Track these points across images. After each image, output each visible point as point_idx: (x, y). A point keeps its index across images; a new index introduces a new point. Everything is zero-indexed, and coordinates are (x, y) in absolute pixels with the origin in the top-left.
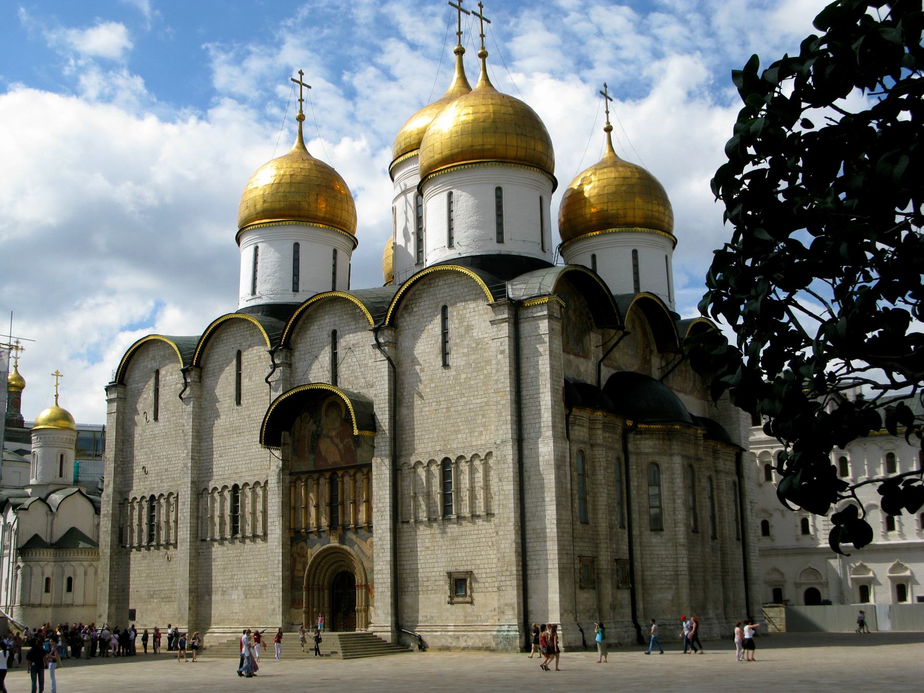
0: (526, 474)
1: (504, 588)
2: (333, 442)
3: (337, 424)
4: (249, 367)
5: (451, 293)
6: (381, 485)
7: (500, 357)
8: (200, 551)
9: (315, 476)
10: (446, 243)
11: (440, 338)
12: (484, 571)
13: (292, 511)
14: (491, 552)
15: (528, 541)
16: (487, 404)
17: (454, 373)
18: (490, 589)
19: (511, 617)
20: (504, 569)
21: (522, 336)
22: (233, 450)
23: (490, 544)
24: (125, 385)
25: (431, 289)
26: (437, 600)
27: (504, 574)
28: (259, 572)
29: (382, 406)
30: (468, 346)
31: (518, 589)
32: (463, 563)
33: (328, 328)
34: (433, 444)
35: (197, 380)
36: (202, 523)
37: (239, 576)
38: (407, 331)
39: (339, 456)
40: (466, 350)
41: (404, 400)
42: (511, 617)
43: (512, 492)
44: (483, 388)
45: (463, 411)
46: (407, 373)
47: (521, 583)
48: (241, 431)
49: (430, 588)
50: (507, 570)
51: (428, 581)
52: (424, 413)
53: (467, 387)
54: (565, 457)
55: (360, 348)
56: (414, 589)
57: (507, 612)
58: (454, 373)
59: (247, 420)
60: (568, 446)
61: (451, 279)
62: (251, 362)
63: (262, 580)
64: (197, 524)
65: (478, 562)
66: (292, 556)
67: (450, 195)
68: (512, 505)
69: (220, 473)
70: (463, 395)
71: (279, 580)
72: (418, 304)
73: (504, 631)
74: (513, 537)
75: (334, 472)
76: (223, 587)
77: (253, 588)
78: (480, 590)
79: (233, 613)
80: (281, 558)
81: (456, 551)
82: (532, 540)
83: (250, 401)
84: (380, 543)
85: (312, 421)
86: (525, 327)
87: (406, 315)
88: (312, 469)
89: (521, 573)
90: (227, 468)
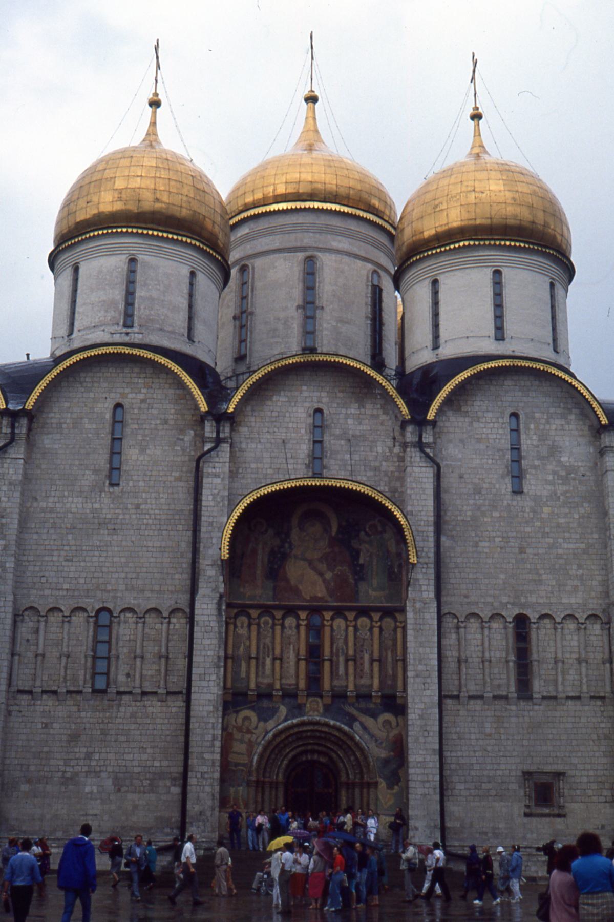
2: (315, 569)
4: (141, 432)
5: (525, 399)
8: (11, 708)
9: (278, 614)
12: (585, 773)
13: (230, 661)
14: (596, 748)
16: (585, 551)
18: (595, 798)
23: (595, 737)
25: (492, 388)
28: (149, 751)
30: (555, 473)
32: (550, 760)
33: (307, 405)
34: (497, 593)
36: (19, 662)
38: (452, 436)
40: (550, 477)
44: (579, 531)
51: (489, 782)
52: (479, 549)
56: (463, 793)
58: (533, 504)
61: (526, 381)
62: (145, 426)
63: (157, 764)
65: (575, 761)
66: (224, 729)
67: (497, 273)
69: (66, 586)
70: (545, 535)
72: (469, 403)
75: (315, 610)
76: (64, 772)
85: (271, 532)
87: (450, 413)
90: (82, 581)
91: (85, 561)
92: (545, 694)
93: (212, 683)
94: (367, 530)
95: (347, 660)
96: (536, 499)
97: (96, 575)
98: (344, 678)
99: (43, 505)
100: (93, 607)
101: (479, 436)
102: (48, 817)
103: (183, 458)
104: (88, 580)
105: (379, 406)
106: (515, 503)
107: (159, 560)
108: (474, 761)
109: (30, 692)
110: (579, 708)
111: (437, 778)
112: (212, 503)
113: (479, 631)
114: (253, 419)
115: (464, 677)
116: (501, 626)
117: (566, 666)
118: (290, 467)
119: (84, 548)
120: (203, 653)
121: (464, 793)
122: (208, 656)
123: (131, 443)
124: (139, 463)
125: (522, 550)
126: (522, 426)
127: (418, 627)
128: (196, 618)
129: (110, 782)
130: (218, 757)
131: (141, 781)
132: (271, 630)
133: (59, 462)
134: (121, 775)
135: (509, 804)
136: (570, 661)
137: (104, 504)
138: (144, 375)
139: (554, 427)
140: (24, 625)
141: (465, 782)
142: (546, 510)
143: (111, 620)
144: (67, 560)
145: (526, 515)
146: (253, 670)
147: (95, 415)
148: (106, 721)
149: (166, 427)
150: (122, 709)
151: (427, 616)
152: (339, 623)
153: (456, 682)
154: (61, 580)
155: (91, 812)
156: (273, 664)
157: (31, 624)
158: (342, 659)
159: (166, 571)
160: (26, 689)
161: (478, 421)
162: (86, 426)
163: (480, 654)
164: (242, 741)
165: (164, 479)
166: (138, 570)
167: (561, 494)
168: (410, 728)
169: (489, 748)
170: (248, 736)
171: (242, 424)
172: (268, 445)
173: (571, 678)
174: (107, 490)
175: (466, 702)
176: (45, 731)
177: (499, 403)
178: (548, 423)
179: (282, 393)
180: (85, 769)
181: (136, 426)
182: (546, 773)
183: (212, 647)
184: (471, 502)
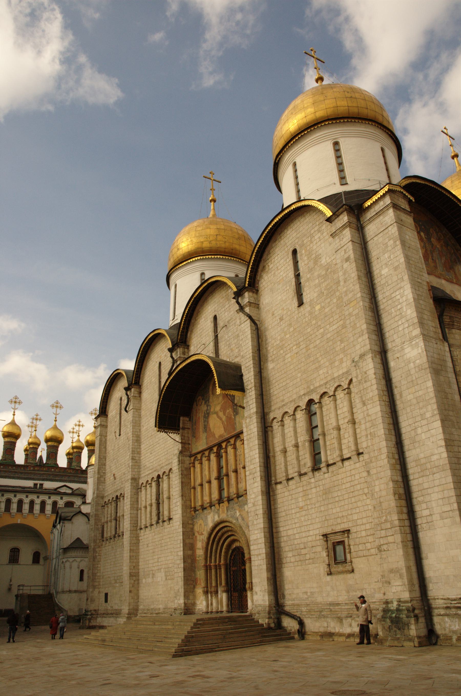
0: (396, 391)
1: (385, 547)
2: (218, 417)
7: (346, 265)
11: (294, 280)
12: (363, 527)
13: (192, 490)
15: (411, 477)
16: (344, 326)
17: (309, 309)
19: (399, 588)
24: (107, 416)
27: (384, 526)
29: (247, 365)
31: (405, 546)
32: (339, 521)
35: (137, 395)
38: (266, 289)
41: (269, 355)
42: (399, 588)
43: (380, 414)
47: (409, 537)
49: (308, 556)
50: (386, 521)
51: (305, 548)
52: (286, 361)
54: (445, 361)
57: (392, 581)
58: (309, 309)
60: (447, 349)
64: (137, 514)
65: (355, 517)
68: (382, 431)
70: (319, 327)
72: (273, 260)
74: (389, 473)
75: (219, 445)
78: (361, 553)
79: (158, 595)
80: (181, 537)
81: (330, 506)
82: (417, 476)
84: (253, 509)
88: (205, 447)
89: (407, 523)
106: (300, 314)
117: (342, 432)
121: (293, 560)
129: (163, 574)
136: (345, 426)
161: (278, 270)
167: (325, 290)
175: (286, 484)
179: (203, 317)
184: (279, 329)
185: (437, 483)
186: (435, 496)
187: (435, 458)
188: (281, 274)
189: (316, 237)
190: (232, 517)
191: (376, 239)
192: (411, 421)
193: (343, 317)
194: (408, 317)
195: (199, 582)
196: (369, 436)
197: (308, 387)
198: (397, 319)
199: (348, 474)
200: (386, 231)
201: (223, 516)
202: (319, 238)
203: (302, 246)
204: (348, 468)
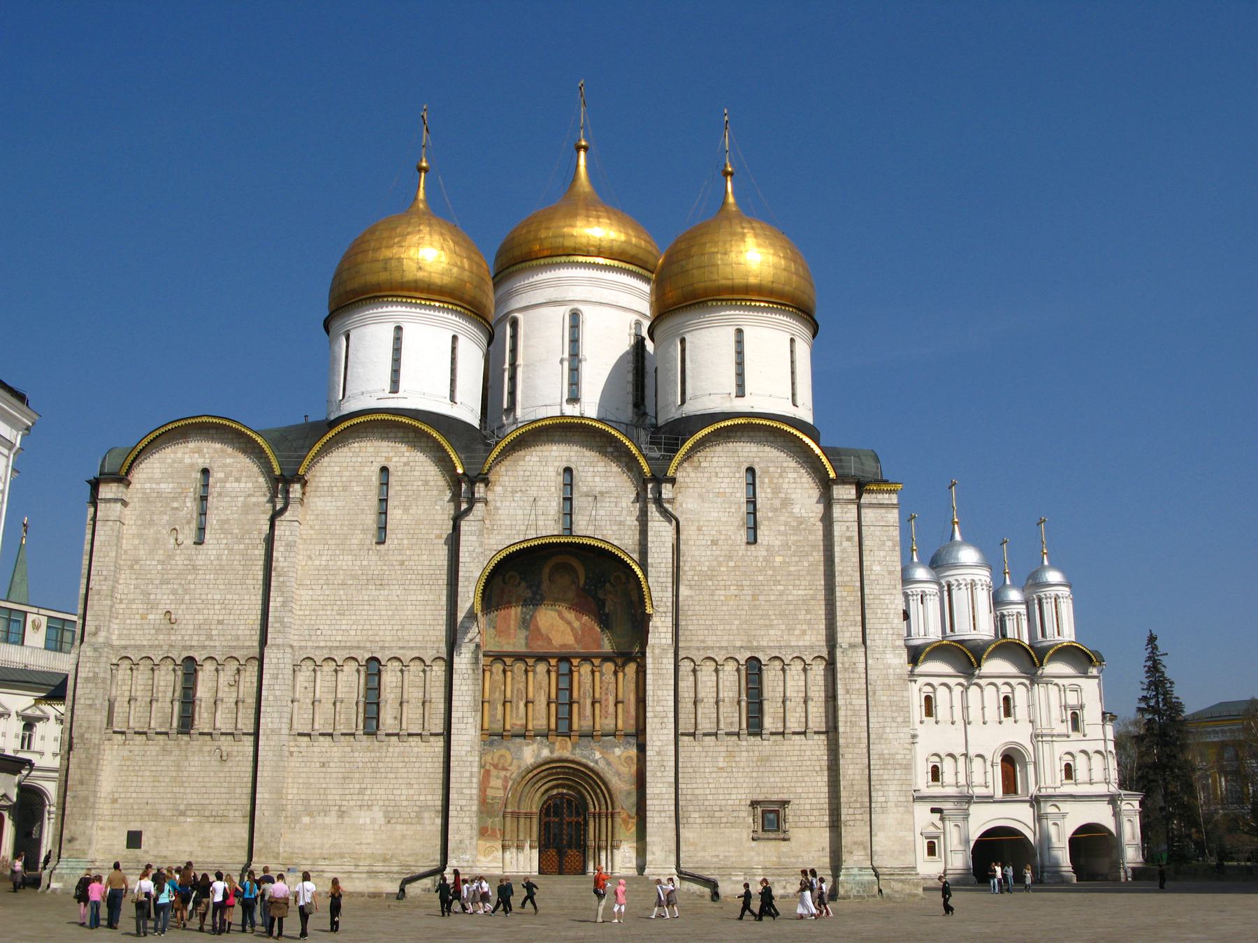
1: (851, 823)
3: (571, 595)
4: (405, 493)
5: (761, 454)
6: (660, 682)
7: (846, 544)
8: (292, 749)
10: (733, 390)
12: (809, 801)
14: (819, 779)
16: (813, 598)
17: (765, 553)
18: (817, 824)
19: (862, 857)
20: (852, 800)
21: (863, 524)
22: (367, 607)
23: (818, 768)
26: (735, 835)
27: (852, 805)
28: (416, 786)
29: (660, 580)
32: (777, 790)
33: (557, 464)
34: (731, 637)
37: (375, 791)
38: (691, 490)
39: (573, 638)
40: (782, 528)
42: (862, 857)
45: (778, 603)
46: (691, 543)
48: (385, 582)
49: (724, 820)
51: (721, 811)
52: (716, 598)
53: (785, 573)
55: (612, 499)
57: (855, 852)
58: (765, 553)
59: (396, 567)
62: (408, 488)
63: (422, 798)
65: (799, 790)
66: (482, 766)
67: (740, 332)
69: (339, 638)
70: (777, 583)
71: (471, 799)
72: (708, 459)
73: (855, 875)
75: (564, 658)
76: (340, 806)
77: (402, 809)
80: (475, 769)
81: (766, 774)
83: (405, 542)
86: (868, 515)
87: (689, 469)
90: (353, 633)
91: (355, 615)
92: (774, 730)
93: (469, 726)
94: (612, 581)
95: (593, 704)
96: (769, 548)
97: (365, 627)
98: (591, 718)
99: (317, 563)
100: (363, 659)
101: (717, 491)
102: (327, 846)
103: (443, 517)
104: (359, 633)
105: (624, 464)
106: (749, 553)
107: (422, 613)
108: (708, 791)
109: (309, 735)
110: (804, 742)
111: (673, 808)
112: (468, 559)
113: (714, 674)
114: (506, 478)
115: (699, 716)
116: (735, 669)
118: (540, 523)
119: (354, 603)
120: (461, 698)
121: (698, 821)
122: (466, 701)
123: (396, 503)
124: (403, 522)
125: (755, 597)
126: (757, 480)
127: (656, 671)
128: (455, 666)
129: (381, 814)
130: (475, 791)
131: (409, 813)
132: (524, 677)
133: (330, 523)
134: (391, 809)
135: (739, 830)
137: (372, 560)
138: (407, 440)
139: (787, 480)
140: (302, 674)
141: (700, 811)
142: (779, 559)
143: (379, 669)
144: (340, 614)
145: (759, 564)
146: (508, 712)
147: (363, 479)
148: (376, 760)
149: (427, 487)
150: (391, 749)
151: (665, 661)
152: (586, 669)
153: (693, 721)
154: (334, 632)
155: (365, 841)
156: (526, 705)
157: (308, 673)
158: (589, 702)
159: (428, 623)
160: (305, 732)
161: (717, 476)
162: (355, 489)
163: (715, 695)
164: (498, 778)
165: (427, 536)
166: (403, 622)
168: (648, 764)
169: (722, 780)
170: (503, 773)
171: (497, 483)
172: (521, 503)
173: (798, 715)
174: (374, 548)
176: (324, 770)
177: (736, 459)
178: (781, 476)
179: (534, 453)
180: (359, 803)
181: (400, 488)
182: (773, 802)
183: (470, 693)
184: (709, 553)
185: (897, 777)
186: (893, 788)
187: (899, 756)
188: (723, 485)
189: (790, 475)
190: (585, 757)
191: (872, 528)
192: (880, 720)
193: (814, 588)
194: (894, 626)
195: (489, 832)
196: (849, 724)
197: (749, 641)
198: (882, 621)
199: (797, 748)
200: (887, 528)
201: (567, 754)
202: (795, 478)
203: (766, 472)
204: (799, 743)
